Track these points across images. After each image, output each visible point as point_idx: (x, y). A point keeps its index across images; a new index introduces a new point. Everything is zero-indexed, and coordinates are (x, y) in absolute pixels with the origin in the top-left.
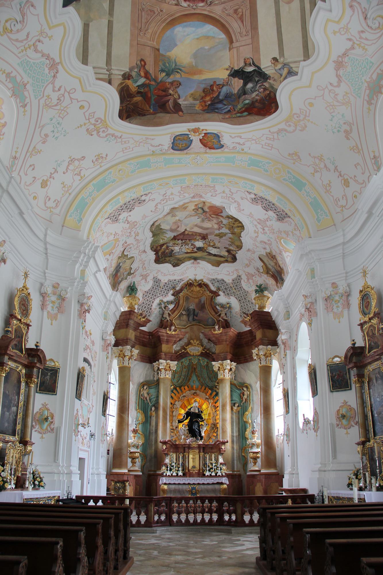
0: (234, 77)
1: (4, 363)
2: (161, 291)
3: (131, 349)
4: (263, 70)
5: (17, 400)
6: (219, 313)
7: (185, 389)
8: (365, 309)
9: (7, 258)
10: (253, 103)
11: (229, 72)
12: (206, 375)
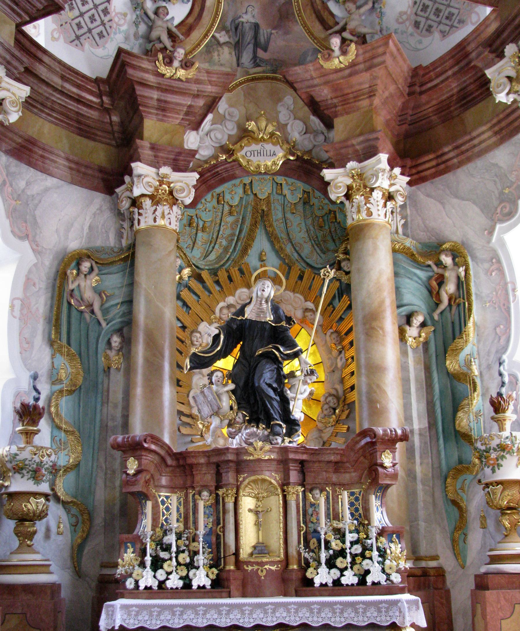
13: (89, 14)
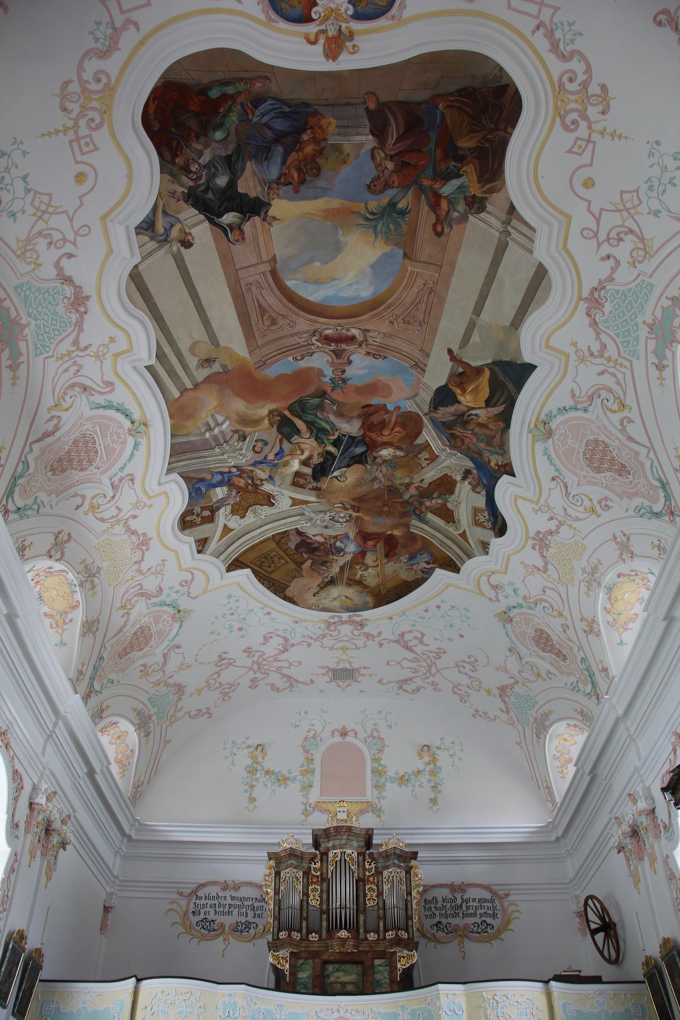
0: (257, 198)
4: (202, 217)
10: (204, 131)
11: (272, 212)
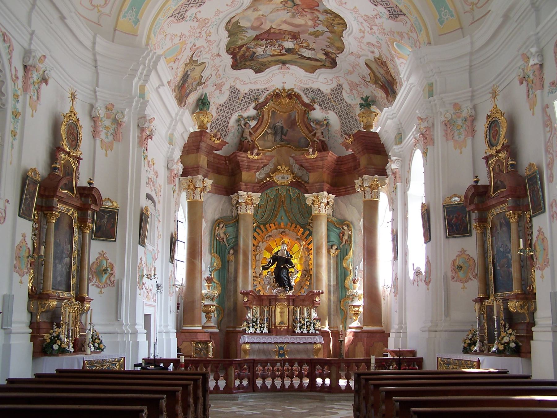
1: (53, 207)
2: (240, 104)
3: (203, 179)
5: (69, 250)
6: (314, 132)
7: (270, 227)
8: (492, 139)
9: (49, 77)
12: (297, 210)
13: (219, 123)
